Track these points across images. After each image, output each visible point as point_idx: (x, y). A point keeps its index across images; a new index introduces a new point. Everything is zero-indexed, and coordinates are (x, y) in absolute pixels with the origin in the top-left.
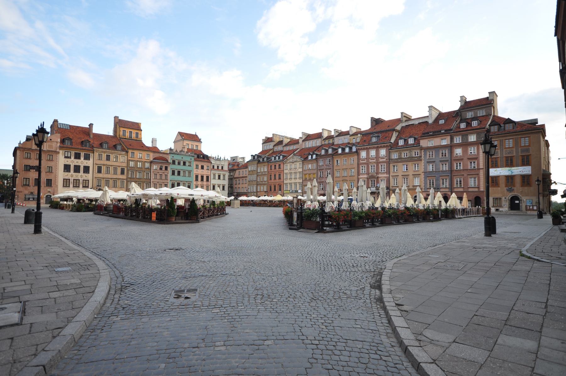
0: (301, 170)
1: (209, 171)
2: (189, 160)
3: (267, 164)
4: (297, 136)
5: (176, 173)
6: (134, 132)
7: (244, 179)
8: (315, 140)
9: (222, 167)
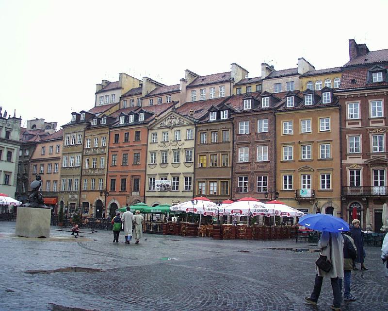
0: (191, 144)
3: (107, 130)
4: (171, 77)
7: (53, 162)
8: (217, 87)
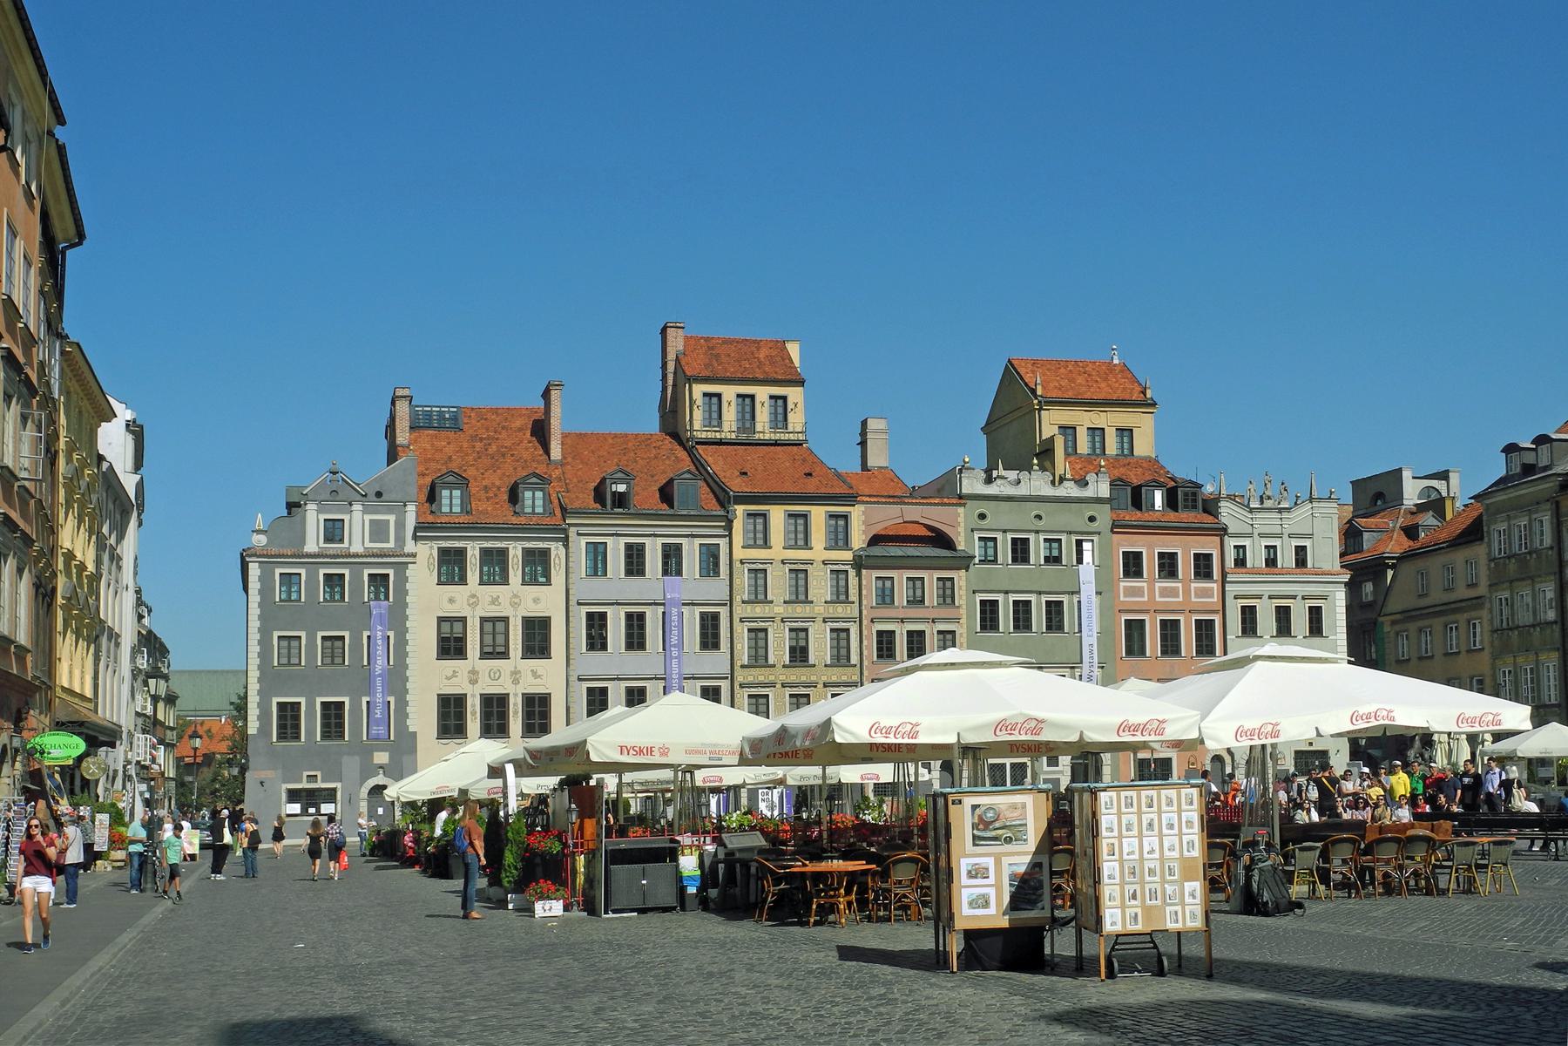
6: (762, 393)
9: (1301, 550)
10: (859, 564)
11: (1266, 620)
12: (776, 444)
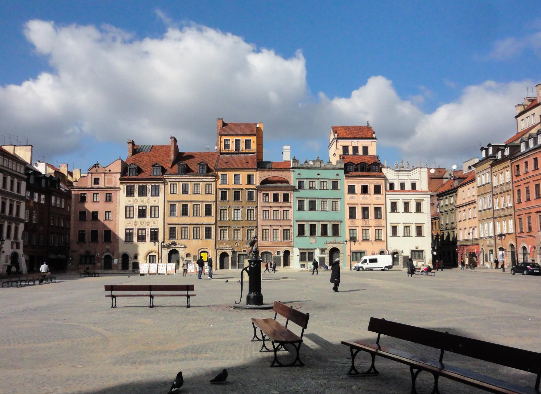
1: (381, 197)
2: (335, 177)
5: (307, 206)
6: (243, 139)
7: (471, 206)
9: (414, 185)
10: (258, 189)
11: (400, 207)
12: (247, 153)
